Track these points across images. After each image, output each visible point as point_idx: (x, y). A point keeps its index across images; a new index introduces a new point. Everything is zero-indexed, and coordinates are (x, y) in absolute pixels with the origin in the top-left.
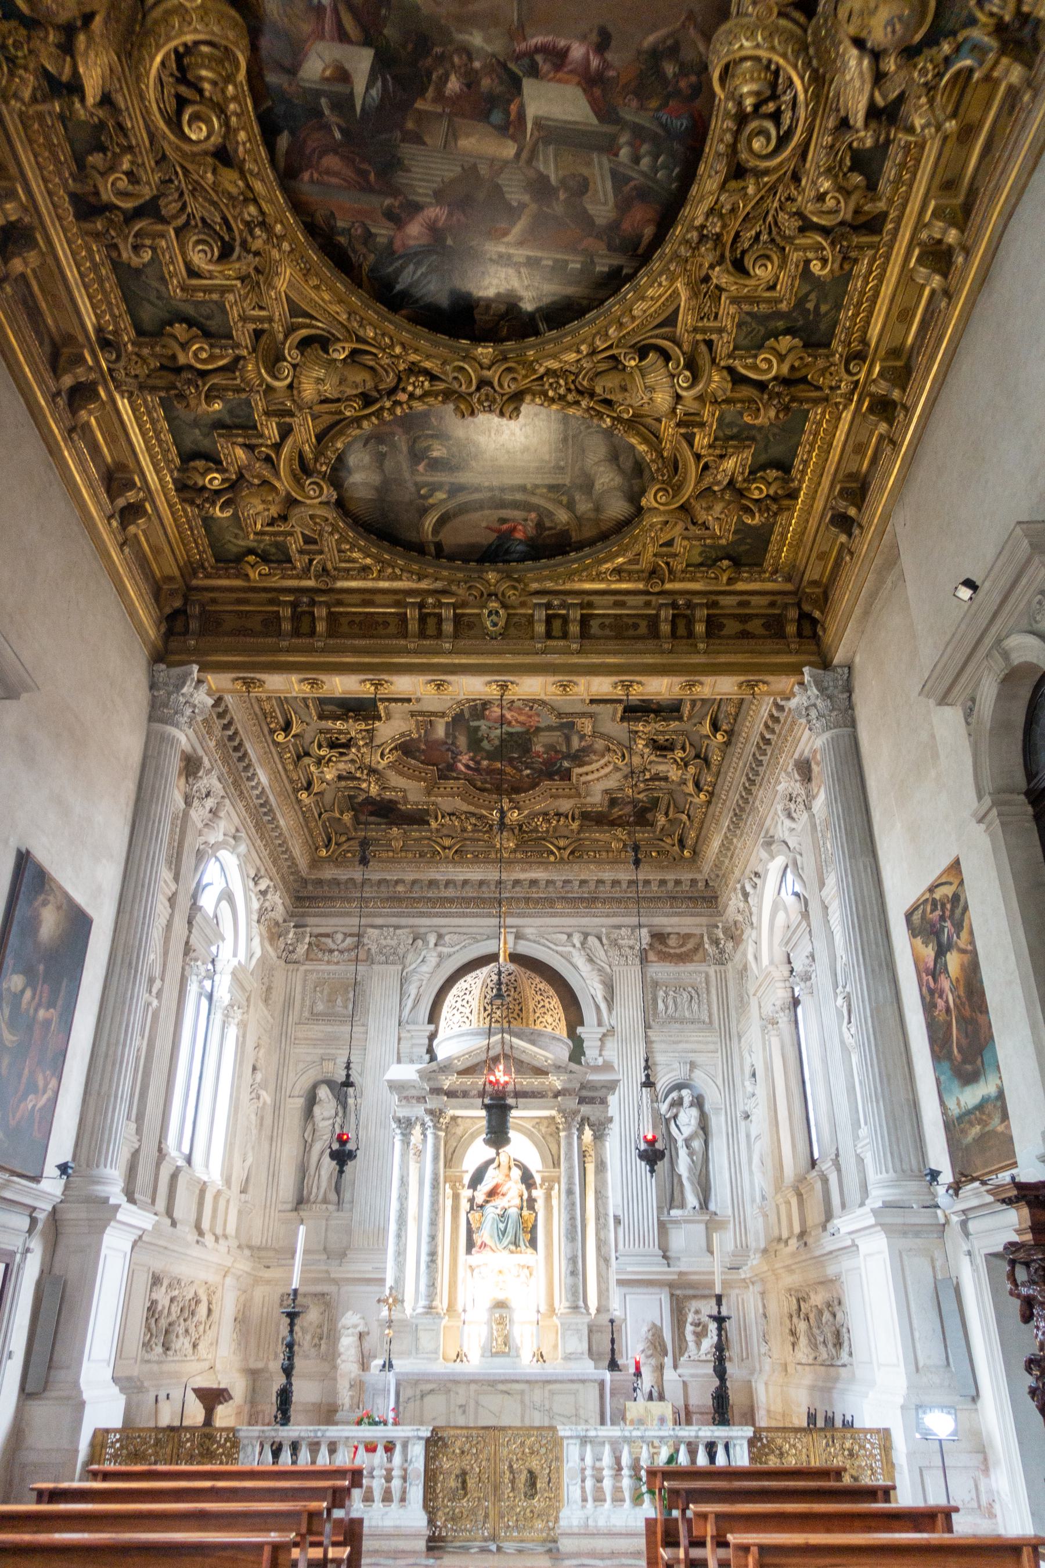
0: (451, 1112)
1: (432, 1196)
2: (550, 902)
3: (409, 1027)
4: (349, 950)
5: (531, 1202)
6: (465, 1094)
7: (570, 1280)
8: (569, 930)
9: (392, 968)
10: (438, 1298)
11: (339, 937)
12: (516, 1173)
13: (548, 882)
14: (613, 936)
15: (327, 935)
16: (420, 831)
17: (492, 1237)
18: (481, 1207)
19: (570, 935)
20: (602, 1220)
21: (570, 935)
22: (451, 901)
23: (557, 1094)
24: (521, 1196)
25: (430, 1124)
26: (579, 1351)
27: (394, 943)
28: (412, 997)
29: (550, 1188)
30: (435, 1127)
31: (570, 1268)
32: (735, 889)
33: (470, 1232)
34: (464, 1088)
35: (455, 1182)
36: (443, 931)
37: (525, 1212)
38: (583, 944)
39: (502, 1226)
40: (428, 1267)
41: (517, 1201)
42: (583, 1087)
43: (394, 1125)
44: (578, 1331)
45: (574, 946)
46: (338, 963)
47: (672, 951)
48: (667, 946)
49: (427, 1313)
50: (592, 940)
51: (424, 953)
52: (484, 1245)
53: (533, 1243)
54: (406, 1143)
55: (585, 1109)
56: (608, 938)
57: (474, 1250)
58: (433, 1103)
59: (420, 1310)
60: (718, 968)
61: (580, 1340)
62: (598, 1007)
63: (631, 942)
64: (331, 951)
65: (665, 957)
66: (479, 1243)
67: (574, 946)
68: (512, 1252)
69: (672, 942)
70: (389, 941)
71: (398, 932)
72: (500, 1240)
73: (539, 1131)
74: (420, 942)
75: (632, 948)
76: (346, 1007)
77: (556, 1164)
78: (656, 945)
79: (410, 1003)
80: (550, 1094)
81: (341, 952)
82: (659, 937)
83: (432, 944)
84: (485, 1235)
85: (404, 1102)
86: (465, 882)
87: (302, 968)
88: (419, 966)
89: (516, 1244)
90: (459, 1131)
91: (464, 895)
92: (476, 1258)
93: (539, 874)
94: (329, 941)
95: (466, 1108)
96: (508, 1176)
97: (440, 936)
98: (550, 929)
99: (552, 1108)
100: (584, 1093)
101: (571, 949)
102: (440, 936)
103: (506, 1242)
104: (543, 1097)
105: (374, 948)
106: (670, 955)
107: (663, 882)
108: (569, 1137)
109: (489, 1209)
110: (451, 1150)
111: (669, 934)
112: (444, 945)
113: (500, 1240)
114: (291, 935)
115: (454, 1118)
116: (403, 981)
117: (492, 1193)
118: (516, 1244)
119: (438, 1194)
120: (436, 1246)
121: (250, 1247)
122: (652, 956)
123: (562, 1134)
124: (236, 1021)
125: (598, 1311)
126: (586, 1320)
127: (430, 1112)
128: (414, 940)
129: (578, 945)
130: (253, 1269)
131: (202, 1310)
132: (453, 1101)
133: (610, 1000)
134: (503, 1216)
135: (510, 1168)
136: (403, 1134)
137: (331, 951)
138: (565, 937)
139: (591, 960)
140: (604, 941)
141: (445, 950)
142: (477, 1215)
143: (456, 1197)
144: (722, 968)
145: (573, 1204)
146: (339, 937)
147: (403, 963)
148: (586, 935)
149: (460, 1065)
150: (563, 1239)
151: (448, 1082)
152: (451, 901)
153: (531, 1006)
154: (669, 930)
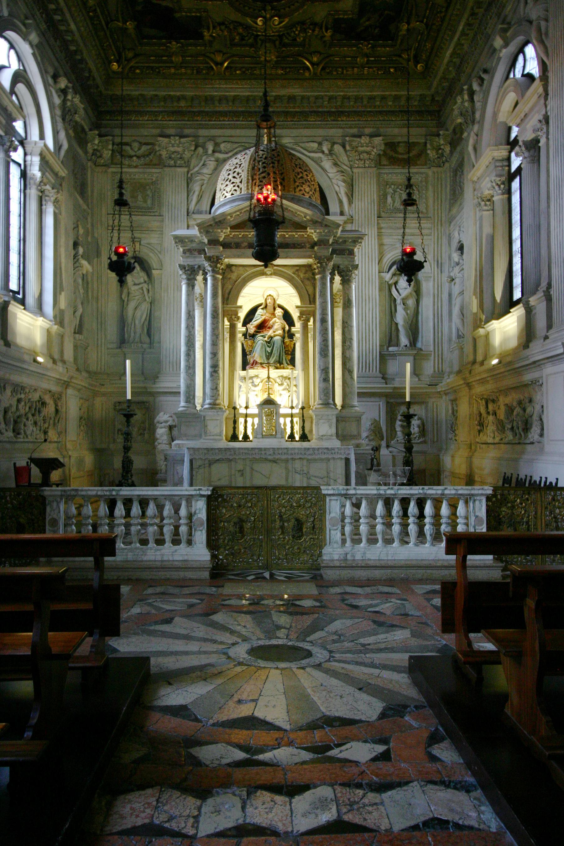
0: (226, 260)
1: (213, 324)
2: (305, 115)
3: (195, 216)
4: (144, 156)
5: (291, 336)
6: (238, 246)
7: (323, 385)
8: (319, 139)
9: (179, 170)
10: (221, 398)
11: (136, 145)
12: (279, 312)
13: (303, 98)
14: (354, 144)
15: (127, 144)
16: (196, 45)
17: (261, 357)
18: (253, 336)
19: (320, 144)
20: (348, 343)
21: (320, 144)
22: (224, 114)
23: (314, 245)
24: (284, 329)
25: (210, 269)
26: (329, 433)
27: (180, 149)
28: (197, 193)
29: (308, 320)
30: (213, 271)
31: (323, 376)
32: (462, 90)
33: (244, 354)
34: (237, 240)
35: (233, 316)
36: (219, 140)
37: (287, 340)
38: (330, 151)
39: (269, 350)
40: (212, 375)
41: (280, 332)
42: (335, 242)
43: (181, 272)
44: (329, 420)
45: (323, 152)
46: (136, 167)
47: (400, 156)
48: (396, 152)
49: (212, 408)
50: (338, 148)
51: (204, 158)
52: (255, 363)
53: (292, 362)
54: (191, 285)
55: (336, 259)
56: (350, 145)
57: (247, 367)
58: (210, 252)
59: (206, 406)
60: (435, 169)
61: (330, 427)
62: (341, 202)
63: (369, 149)
64: (131, 157)
65: (394, 161)
66: (252, 362)
67: (323, 152)
68: (277, 368)
69: (401, 149)
70: (176, 149)
71: (183, 140)
72: (268, 358)
73: (298, 276)
74: (200, 150)
75: (368, 153)
76: (145, 202)
77: (312, 301)
78: (389, 152)
79: (195, 199)
80: (308, 245)
81: (138, 157)
82: (391, 145)
83: (210, 152)
84: (257, 355)
85: (188, 254)
86: (235, 98)
87: (111, 170)
88: (200, 169)
89: (281, 363)
90: (234, 276)
91: (235, 109)
92: (251, 372)
93: (296, 90)
94: (128, 148)
95: (239, 257)
96: (273, 314)
97: (217, 145)
98: (305, 139)
99: (310, 257)
100: (337, 247)
101: (320, 155)
102: (217, 145)
103: (272, 361)
104: (302, 247)
105: (164, 153)
106: (398, 159)
107: (397, 98)
108: (323, 278)
109: (259, 338)
110: (227, 291)
111: (399, 143)
112: (220, 152)
113: (268, 358)
114: (96, 142)
115: (230, 266)
116: (189, 181)
117: (262, 326)
118: (281, 363)
119: (218, 322)
120: (217, 361)
121: (88, 372)
122: (384, 161)
123: (317, 277)
124: (53, 199)
125: (343, 407)
126: (336, 412)
127: (209, 259)
128: (196, 147)
129: (326, 152)
130: (91, 385)
131: (50, 409)
132: (228, 251)
133: (350, 196)
134: (270, 342)
135: (275, 309)
136: (188, 279)
137: (131, 157)
138: (315, 145)
139: (336, 164)
140: (348, 148)
141: (221, 156)
142: (250, 342)
143: (233, 327)
144: (440, 169)
145: (326, 329)
146: (136, 145)
147: (188, 166)
148: (334, 144)
149: (233, 221)
150: (317, 355)
151: (223, 234)
152: (224, 114)
153: (292, 176)
154: (399, 139)
